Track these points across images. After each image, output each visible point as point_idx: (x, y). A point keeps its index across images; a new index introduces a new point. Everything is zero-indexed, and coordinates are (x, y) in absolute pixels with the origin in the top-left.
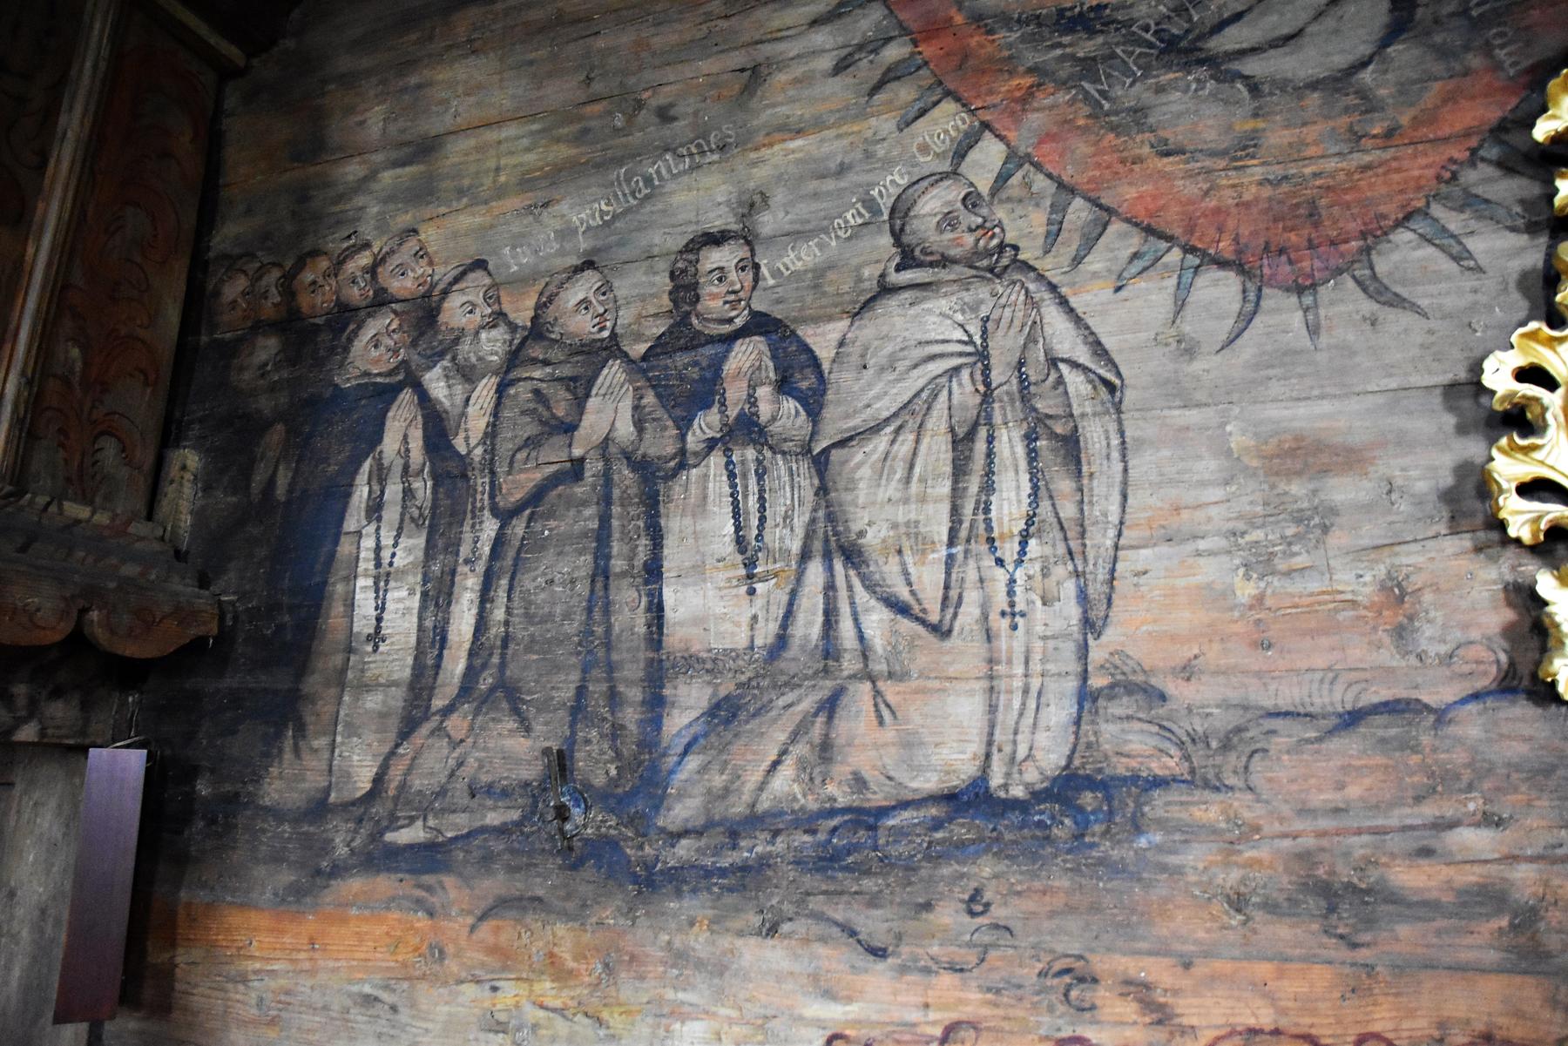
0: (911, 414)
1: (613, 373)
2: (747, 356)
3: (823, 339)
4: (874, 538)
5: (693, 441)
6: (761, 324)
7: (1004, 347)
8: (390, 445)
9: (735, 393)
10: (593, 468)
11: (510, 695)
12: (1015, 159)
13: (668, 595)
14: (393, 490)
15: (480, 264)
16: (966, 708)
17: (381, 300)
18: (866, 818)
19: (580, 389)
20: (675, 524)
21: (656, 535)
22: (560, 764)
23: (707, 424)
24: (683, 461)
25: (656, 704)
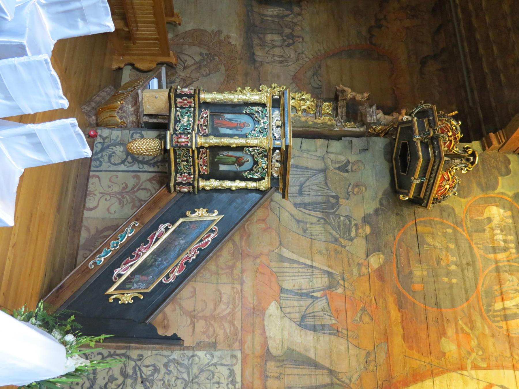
0: (285, 53)
1: (290, 31)
2: (291, 41)
3: (292, 47)
4: (274, 49)
5: (284, 37)
6: (294, 43)
7: (290, 60)
8: (286, 11)
9: (288, 40)
10: (282, 29)
11: (262, 22)
12: (307, 62)
13: (270, 35)
14: (281, 12)
15: (304, 19)
16: (260, 54)
17: (301, 10)
18: (252, 47)
19: (290, 28)
20: (276, 35)
21: (276, 34)
22: (256, 26)
23: (285, 38)
24: (282, 36)
25: (261, 33)
